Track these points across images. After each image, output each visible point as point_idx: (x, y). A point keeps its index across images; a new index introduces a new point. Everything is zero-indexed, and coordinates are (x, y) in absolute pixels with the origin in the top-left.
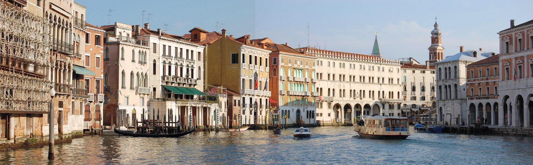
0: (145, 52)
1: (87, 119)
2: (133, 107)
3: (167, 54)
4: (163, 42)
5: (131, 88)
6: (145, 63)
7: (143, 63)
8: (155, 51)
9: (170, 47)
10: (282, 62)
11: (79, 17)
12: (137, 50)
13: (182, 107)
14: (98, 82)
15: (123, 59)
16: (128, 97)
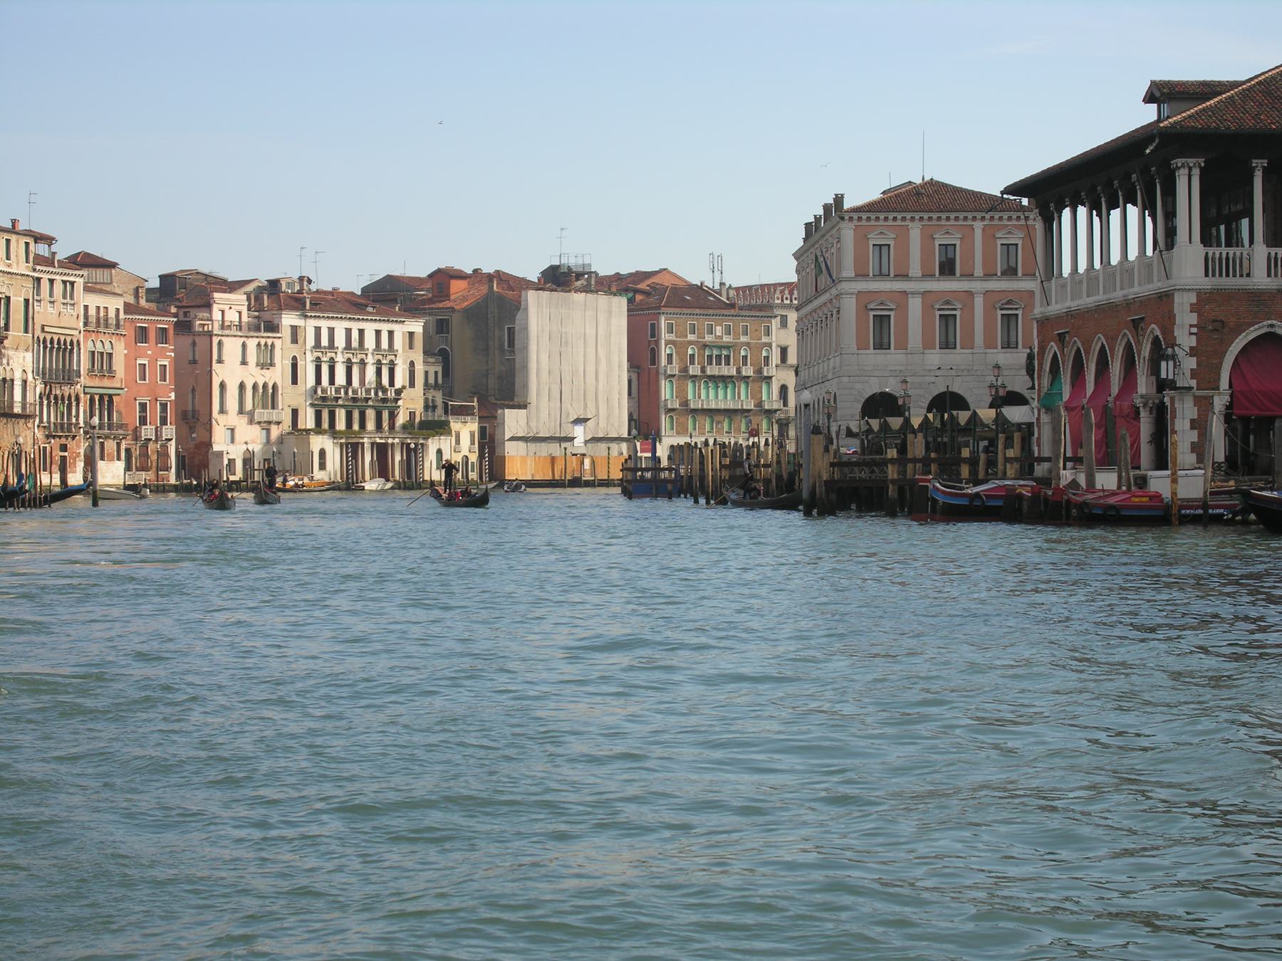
0: (273, 345)
1: (128, 468)
2: (245, 447)
3: (325, 342)
4: (311, 324)
5: (241, 411)
6: (272, 364)
7: (267, 364)
8: (294, 340)
9: (331, 330)
10: (670, 331)
11: (112, 314)
12: (252, 344)
13: (347, 444)
14: (164, 406)
15: (220, 361)
16: (232, 430)
